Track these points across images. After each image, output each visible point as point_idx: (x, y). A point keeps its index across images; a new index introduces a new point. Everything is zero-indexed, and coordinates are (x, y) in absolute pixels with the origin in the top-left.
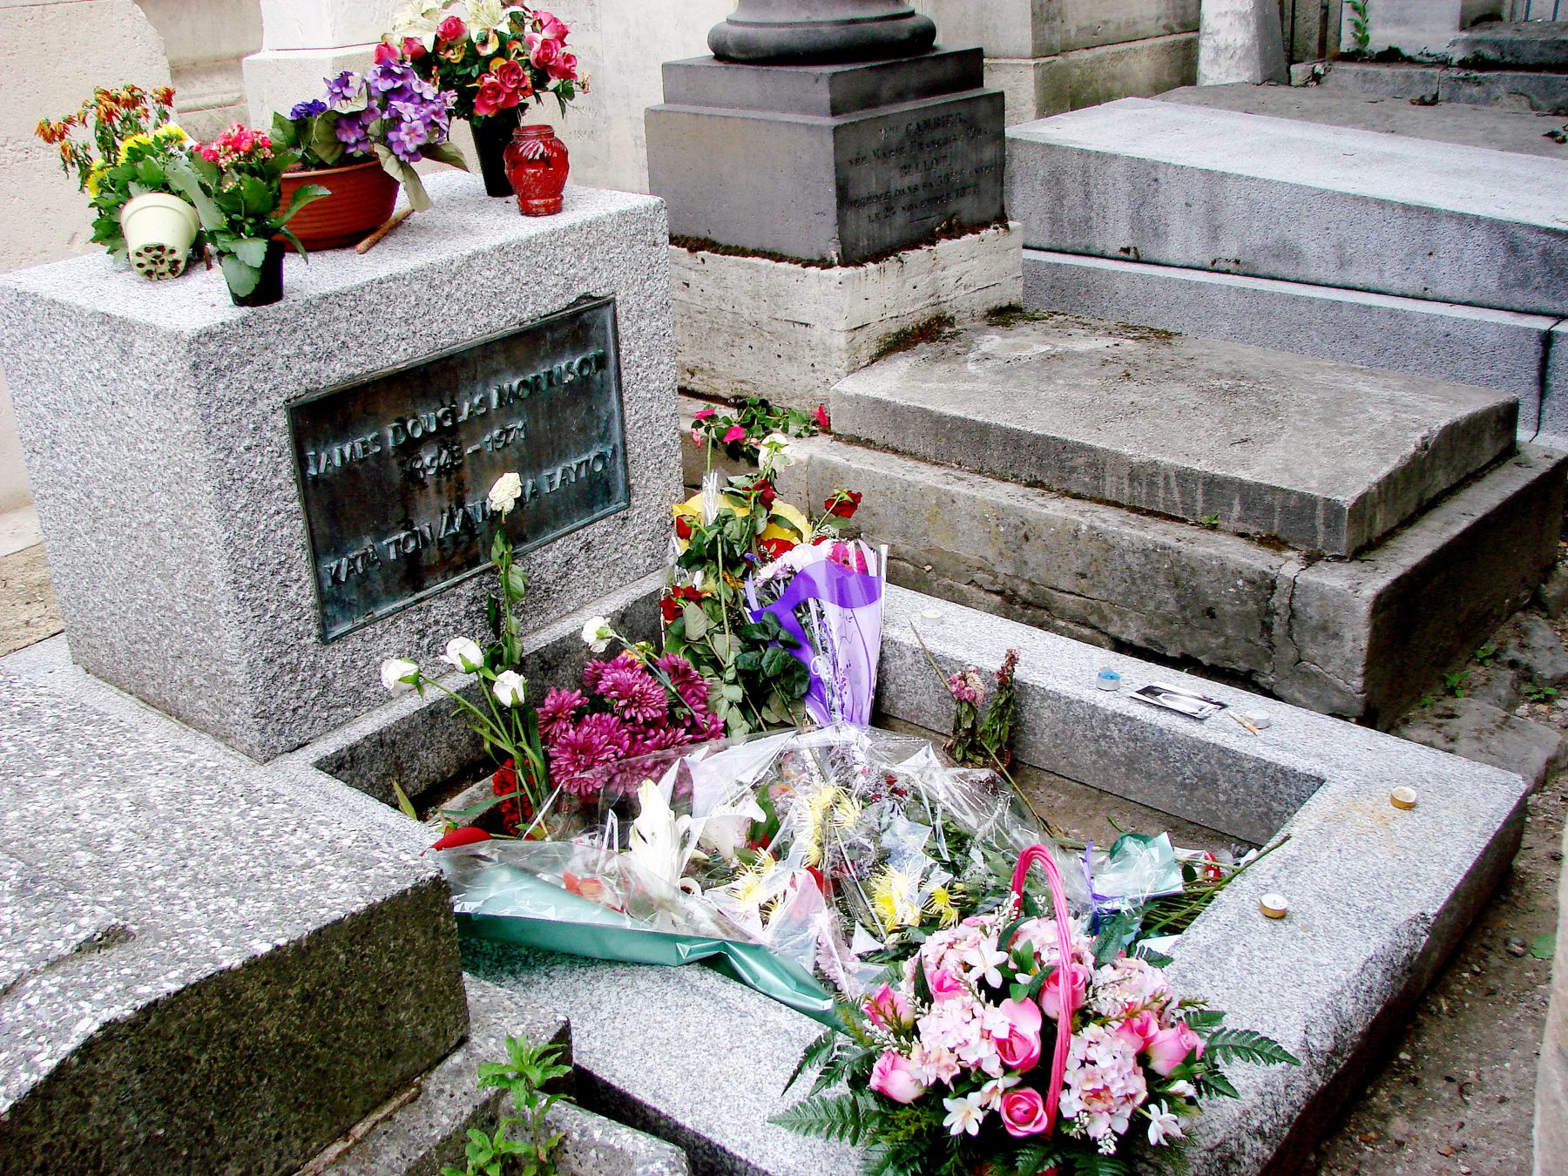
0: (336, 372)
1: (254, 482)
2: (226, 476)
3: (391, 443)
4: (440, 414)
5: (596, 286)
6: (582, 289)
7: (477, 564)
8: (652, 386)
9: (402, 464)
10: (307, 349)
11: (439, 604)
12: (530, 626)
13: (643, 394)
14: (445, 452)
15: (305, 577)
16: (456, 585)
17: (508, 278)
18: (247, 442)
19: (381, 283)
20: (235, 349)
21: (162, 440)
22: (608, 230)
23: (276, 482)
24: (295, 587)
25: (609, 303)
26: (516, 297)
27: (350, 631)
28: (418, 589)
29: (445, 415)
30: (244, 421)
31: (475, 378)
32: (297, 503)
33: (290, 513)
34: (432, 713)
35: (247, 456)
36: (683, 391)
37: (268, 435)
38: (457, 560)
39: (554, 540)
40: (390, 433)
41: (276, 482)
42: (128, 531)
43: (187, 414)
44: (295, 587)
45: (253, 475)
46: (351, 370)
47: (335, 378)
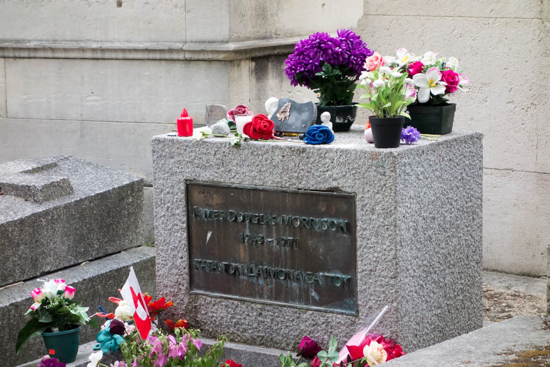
5: (347, 185)
6: (334, 184)
8: (376, 255)
13: (371, 256)
18: (168, 190)
20: (167, 150)
23: (177, 212)
24: (180, 260)
26: (296, 174)
30: (169, 181)
35: (168, 196)
39: (308, 310)
41: (177, 212)
45: (169, 205)
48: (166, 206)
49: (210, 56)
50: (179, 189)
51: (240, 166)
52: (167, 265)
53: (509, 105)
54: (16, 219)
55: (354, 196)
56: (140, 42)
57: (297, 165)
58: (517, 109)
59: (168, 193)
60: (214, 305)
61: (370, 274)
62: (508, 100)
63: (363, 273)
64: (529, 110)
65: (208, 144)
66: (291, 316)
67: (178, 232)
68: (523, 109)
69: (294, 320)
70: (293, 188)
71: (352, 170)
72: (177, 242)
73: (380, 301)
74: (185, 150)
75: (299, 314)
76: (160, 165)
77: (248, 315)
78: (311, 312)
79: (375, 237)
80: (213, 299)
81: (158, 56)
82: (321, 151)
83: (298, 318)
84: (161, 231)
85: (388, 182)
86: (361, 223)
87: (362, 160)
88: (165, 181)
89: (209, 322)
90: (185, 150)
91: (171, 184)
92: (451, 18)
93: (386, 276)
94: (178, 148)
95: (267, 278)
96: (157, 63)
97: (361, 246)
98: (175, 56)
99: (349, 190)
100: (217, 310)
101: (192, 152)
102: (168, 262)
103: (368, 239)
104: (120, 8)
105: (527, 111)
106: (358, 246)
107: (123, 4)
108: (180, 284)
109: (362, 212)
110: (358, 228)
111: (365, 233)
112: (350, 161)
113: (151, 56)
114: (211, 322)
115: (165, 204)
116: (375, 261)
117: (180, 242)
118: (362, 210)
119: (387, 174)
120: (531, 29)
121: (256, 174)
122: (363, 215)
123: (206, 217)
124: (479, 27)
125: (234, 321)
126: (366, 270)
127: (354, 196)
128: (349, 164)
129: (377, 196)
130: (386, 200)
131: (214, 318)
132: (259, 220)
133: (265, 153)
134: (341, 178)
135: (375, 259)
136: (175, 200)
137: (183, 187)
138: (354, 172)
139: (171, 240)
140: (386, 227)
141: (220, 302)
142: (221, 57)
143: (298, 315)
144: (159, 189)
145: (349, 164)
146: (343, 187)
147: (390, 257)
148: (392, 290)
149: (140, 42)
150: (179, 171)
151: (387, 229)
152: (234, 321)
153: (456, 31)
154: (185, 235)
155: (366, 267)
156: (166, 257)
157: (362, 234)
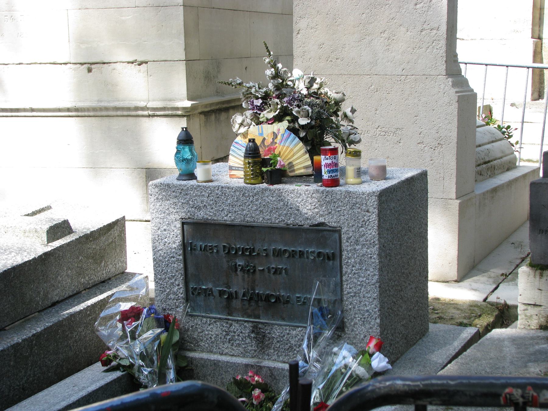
0: (201, 215)
1: (166, 242)
2: (157, 236)
6: (321, 220)
7: (259, 318)
8: (361, 279)
9: (228, 262)
10: (190, 202)
11: (236, 325)
12: (281, 359)
13: (355, 281)
15: (181, 286)
16: (246, 321)
17: (282, 203)
18: (165, 227)
19: (222, 188)
22: (338, 197)
24: (177, 287)
25: (337, 231)
26: (285, 212)
27: (198, 316)
28: (229, 314)
30: (165, 220)
31: (264, 240)
32: (181, 257)
33: (178, 260)
34: (215, 364)
35: (164, 232)
36: (49, 208)
37: (173, 228)
38: (249, 311)
39: (298, 327)
44: (177, 287)
46: (206, 216)
49: (170, 112)
50: (175, 226)
51: (232, 206)
52: (165, 291)
54: (31, 259)
55: (340, 230)
56: (109, 102)
57: (286, 204)
58: (426, 148)
59: (165, 230)
60: (209, 325)
61: (354, 296)
62: (419, 141)
63: (349, 295)
64: (436, 149)
66: (282, 333)
68: (432, 148)
69: (284, 336)
70: (282, 225)
71: (337, 207)
73: (365, 318)
74: (181, 193)
75: (289, 330)
76: (157, 207)
77: (242, 332)
78: (300, 328)
79: (359, 264)
80: (208, 320)
81: (125, 113)
82: (308, 192)
83: (288, 334)
85: (371, 217)
86: (346, 253)
87: (347, 199)
88: (162, 220)
89: (205, 339)
90: (181, 193)
92: (369, 76)
93: (370, 297)
94: (174, 192)
95: (258, 301)
96: (125, 118)
97: (346, 272)
98: (140, 113)
99: (335, 225)
100: (212, 328)
101: (187, 194)
102: (166, 288)
103: (353, 266)
104: (90, 74)
105: (434, 150)
106: (344, 272)
107: (93, 70)
108: (177, 307)
109: (347, 244)
110: (344, 257)
111: (350, 261)
112: (335, 200)
113: (119, 113)
114: (207, 339)
116: (360, 285)
118: (348, 242)
119: (370, 210)
120: (437, 83)
121: (247, 213)
122: (348, 246)
123: (201, 249)
124: (392, 83)
125: (229, 337)
126: (351, 293)
127: (340, 230)
128: (335, 202)
129: (361, 230)
130: (369, 232)
131: (210, 336)
132: (250, 252)
133: (255, 195)
134: (327, 214)
135: (359, 283)
136: (171, 236)
137: (179, 225)
138: (339, 209)
140: (369, 256)
141: (215, 322)
142: (180, 113)
143: (288, 331)
144: (157, 227)
145: (335, 202)
146: (329, 222)
147: (374, 281)
148: (375, 308)
149: (109, 102)
150: (175, 211)
151: (371, 257)
152: (229, 337)
153: (373, 87)
154: (182, 265)
155: (351, 290)
156: (164, 285)
157: (347, 262)
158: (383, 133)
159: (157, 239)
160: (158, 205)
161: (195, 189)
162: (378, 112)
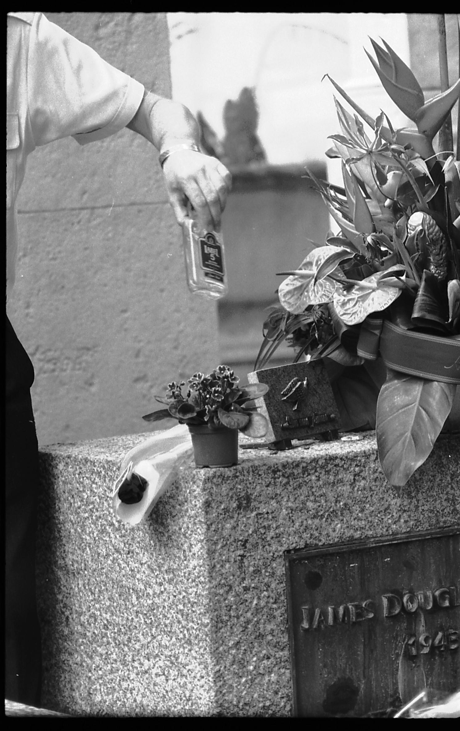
2: (223, 612)
3: (385, 613)
4: (437, 593)
14: (440, 634)
21: (170, 581)
23: (269, 627)
29: (442, 595)
40: (385, 602)
41: (269, 627)
42: (125, 685)
43: (195, 549)
47: (335, 537)
48: (242, 619)
53: (139, 385)
62: (136, 375)
65: (337, 461)
67: (270, 673)
72: (269, 694)
84: (230, 682)
91: (251, 569)
115: (238, 617)
117: (276, 693)
139: (256, 695)
158: (51, 366)
159: (225, 618)
160: (228, 526)
161: (322, 467)
162: (31, 310)
